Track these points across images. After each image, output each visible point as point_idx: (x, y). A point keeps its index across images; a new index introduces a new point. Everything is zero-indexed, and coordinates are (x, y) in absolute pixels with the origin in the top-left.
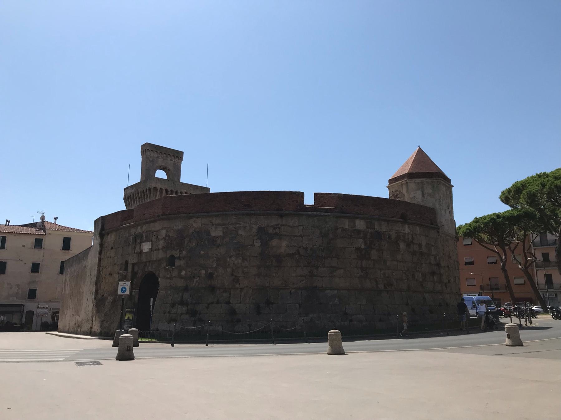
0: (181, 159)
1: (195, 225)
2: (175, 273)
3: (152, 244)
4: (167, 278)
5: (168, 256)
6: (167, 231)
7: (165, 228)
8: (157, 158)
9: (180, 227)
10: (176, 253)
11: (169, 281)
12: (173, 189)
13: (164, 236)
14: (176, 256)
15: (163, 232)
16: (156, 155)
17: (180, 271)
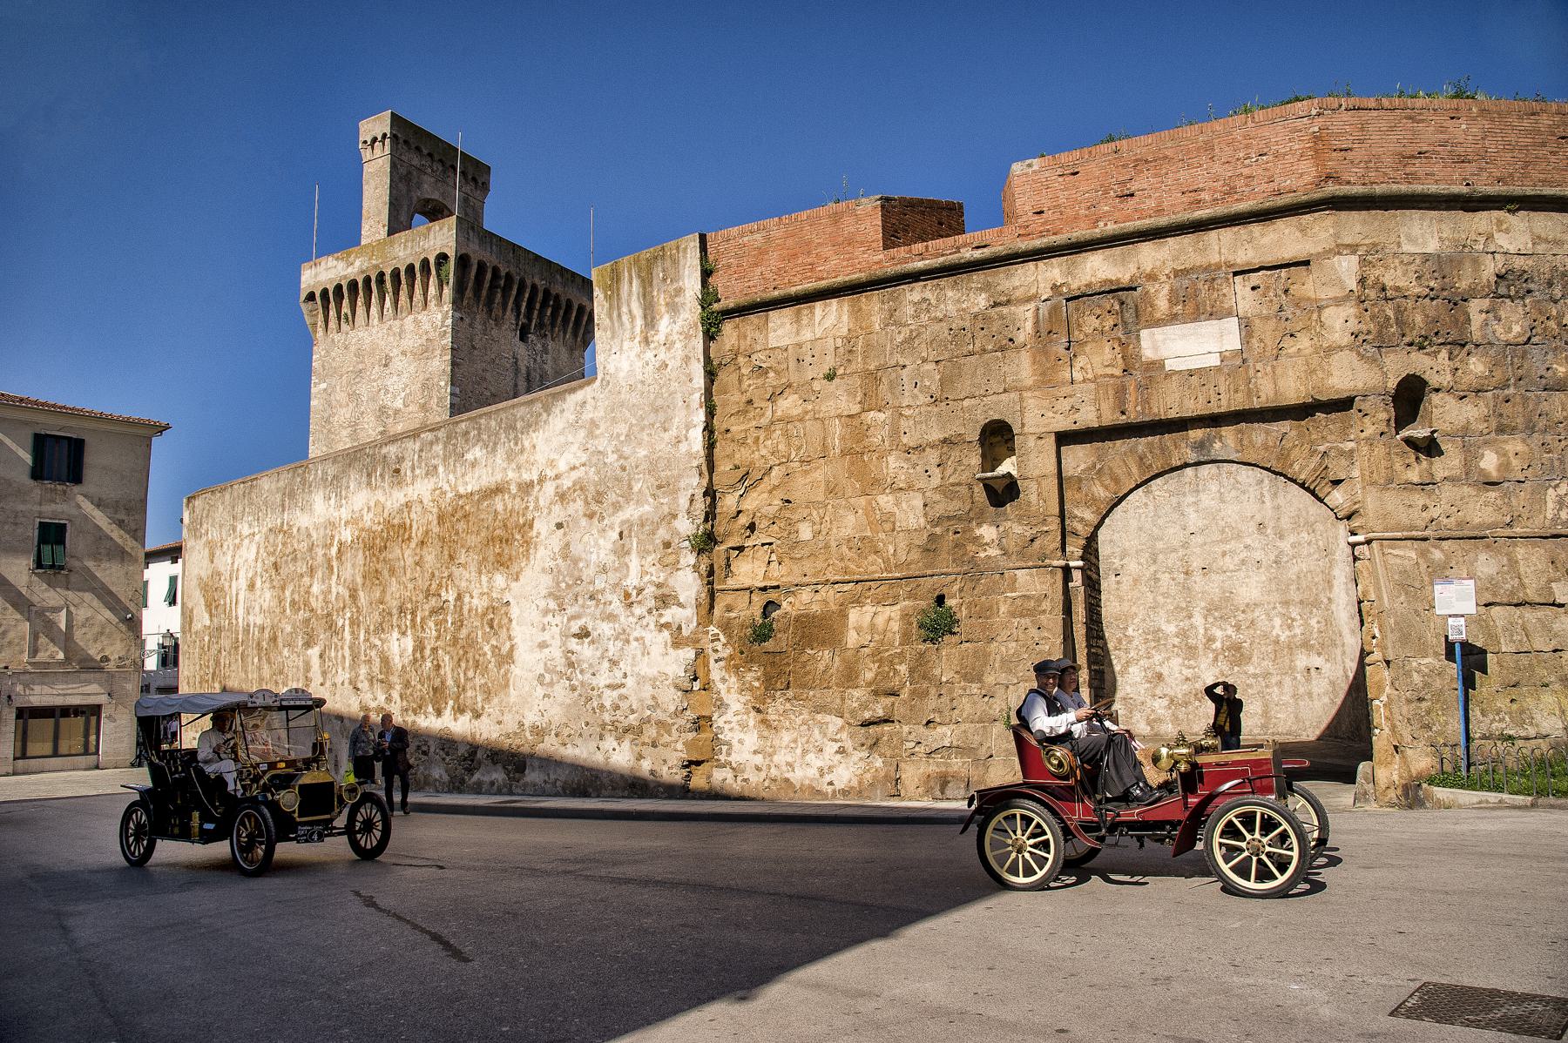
0: (485, 188)
1: (1502, 241)
2: (1449, 463)
3: (1246, 326)
4: (1410, 486)
5: (1392, 384)
6: (1363, 262)
7: (1353, 249)
8: (421, 170)
9: (1432, 246)
10: (1434, 367)
11: (1419, 499)
12: (513, 270)
13: (1354, 287)
14: (1433, 380)
15: (1347, 268)
16: (416, 162)
17: (1471, 456)
